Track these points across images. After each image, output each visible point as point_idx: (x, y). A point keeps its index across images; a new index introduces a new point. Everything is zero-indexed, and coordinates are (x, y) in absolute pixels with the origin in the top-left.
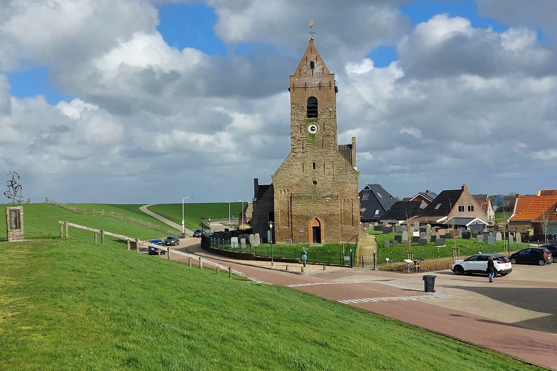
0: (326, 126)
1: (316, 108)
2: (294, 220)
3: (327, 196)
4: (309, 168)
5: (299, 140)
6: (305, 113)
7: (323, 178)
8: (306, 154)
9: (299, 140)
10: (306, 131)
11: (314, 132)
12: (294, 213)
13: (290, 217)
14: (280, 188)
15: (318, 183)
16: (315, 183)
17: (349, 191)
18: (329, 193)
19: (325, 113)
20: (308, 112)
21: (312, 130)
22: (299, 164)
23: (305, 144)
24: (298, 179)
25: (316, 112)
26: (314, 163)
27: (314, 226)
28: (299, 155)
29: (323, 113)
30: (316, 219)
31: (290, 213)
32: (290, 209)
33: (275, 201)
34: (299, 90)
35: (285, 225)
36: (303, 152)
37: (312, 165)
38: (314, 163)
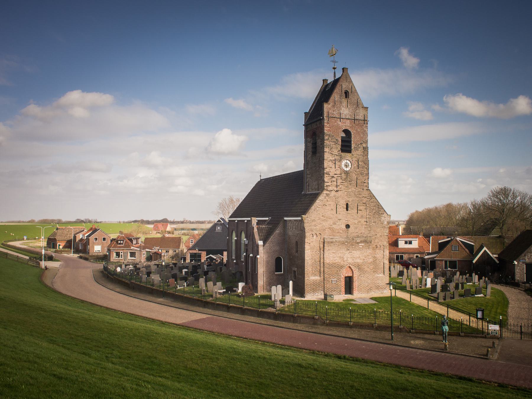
0: (360, 163)
1: (350, 142)
2: (326, 270)
3: (361, 242)
4: (342, 209)
5: (333, 177)
6: (339, 147)
7: (356, 222)
8: (340, 193)
9: (333, 177)
10: (340, 167)
11: (348, 169)
12: (327, 261)
13: (322, 265)
14: (312, 231)
15: (351, 226)
16: (348, 226)
17: (381, 236)
18: (363, 239)
19: (360, 149)
20: (342, 146)
21: (346, 166)
22: (333, 204)
23: (339, 181)
24: (330, 222)
25: (350, 146)
26: (347, 205)
27: (346, 275)
28: (333, 193)
29: (356, 149)
30: (350, 267)
31: (322, 261)
32: (322, 256)
33: (307, 247)
34: (333, 120)
35: (316, 275)
36: (337, 191)
37: (345, 207)
38: (347, 205)
